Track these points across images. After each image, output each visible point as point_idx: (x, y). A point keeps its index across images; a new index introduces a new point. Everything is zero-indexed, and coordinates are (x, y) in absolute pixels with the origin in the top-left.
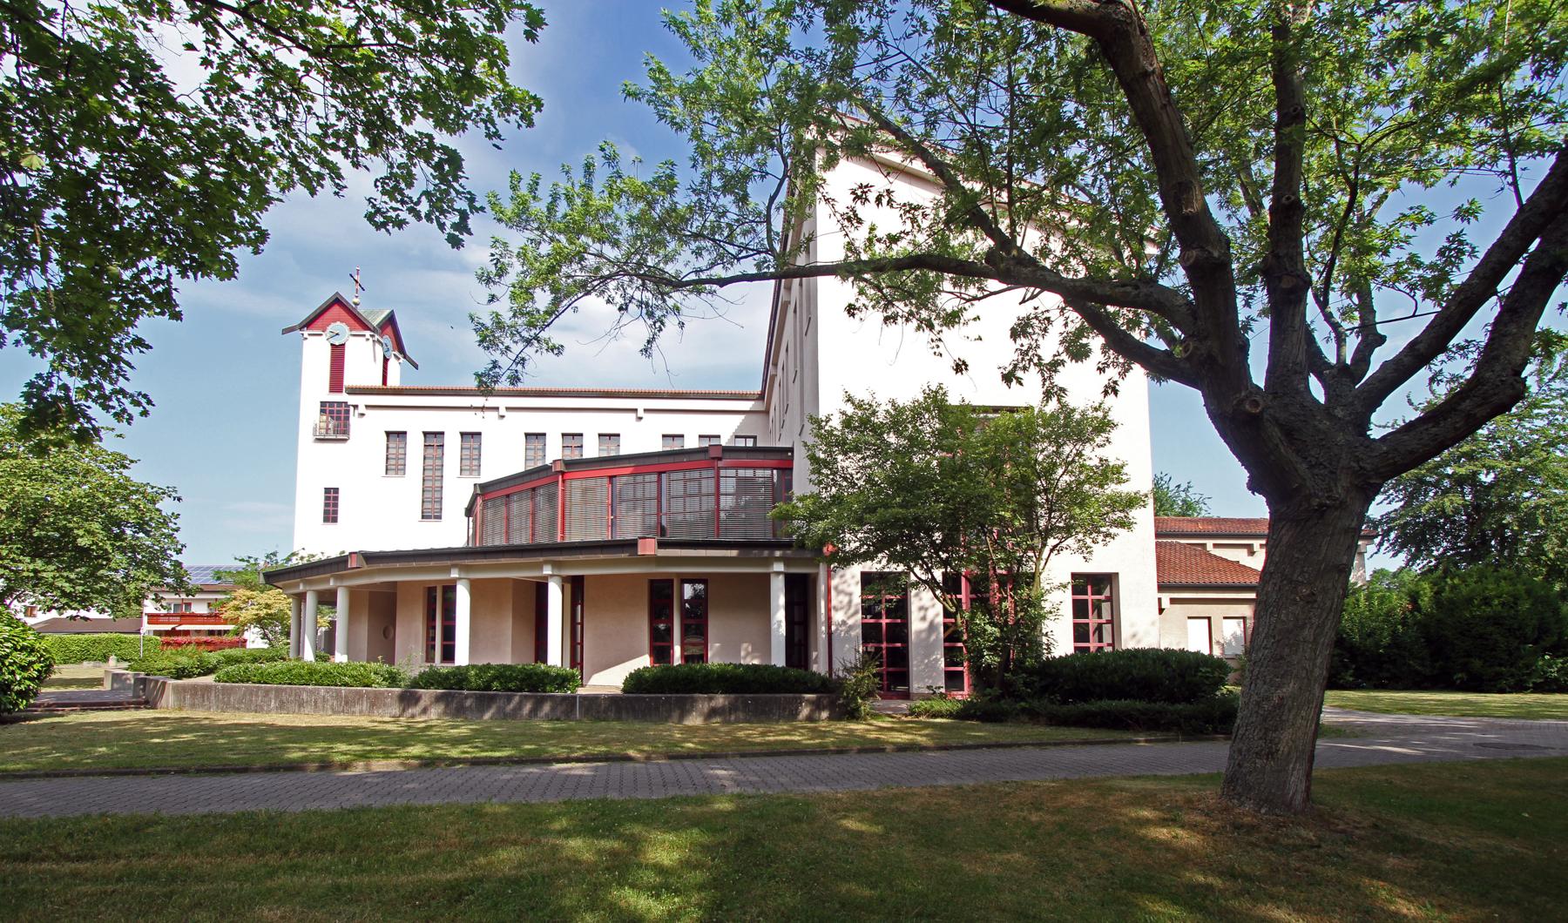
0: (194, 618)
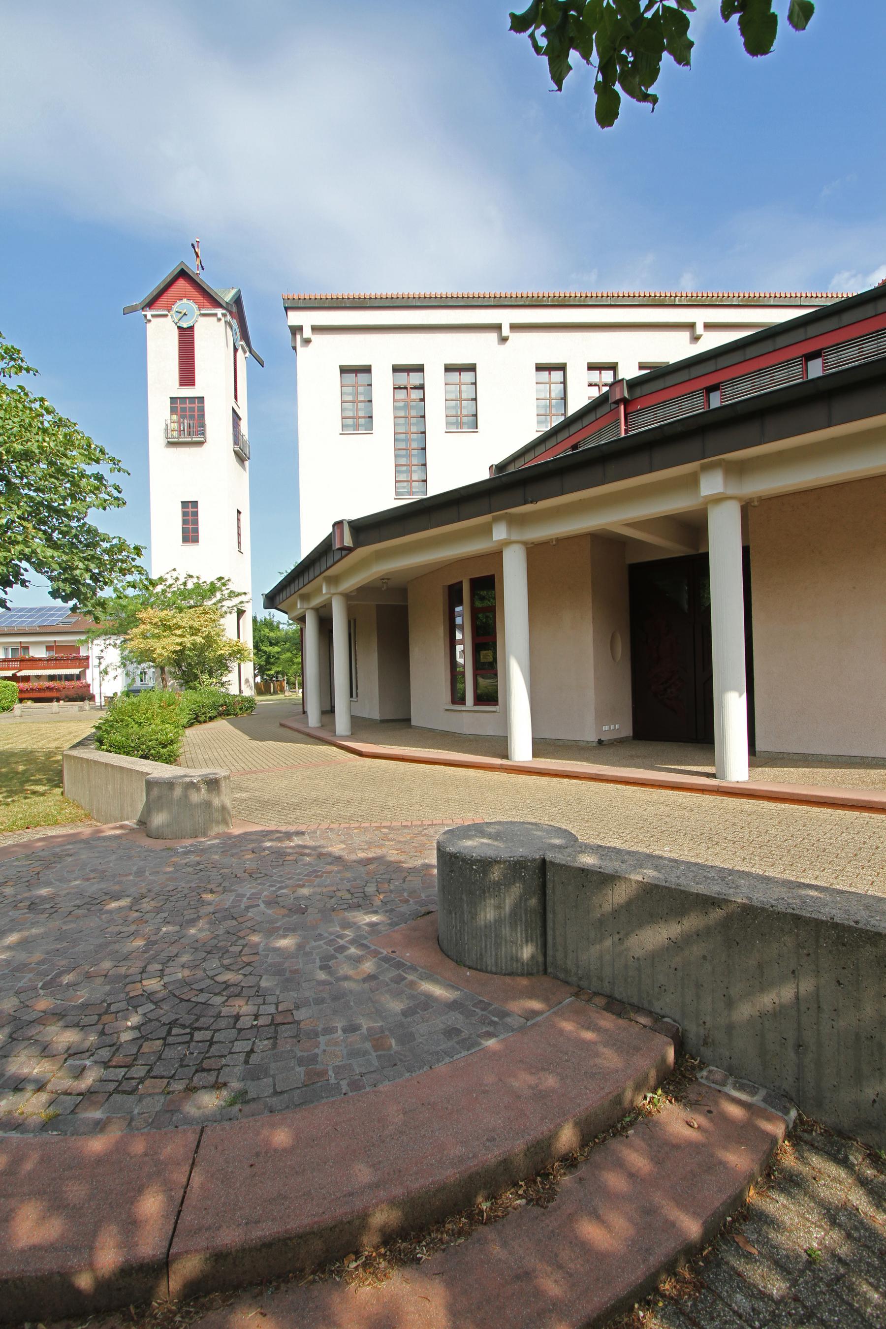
0: (34, 662)
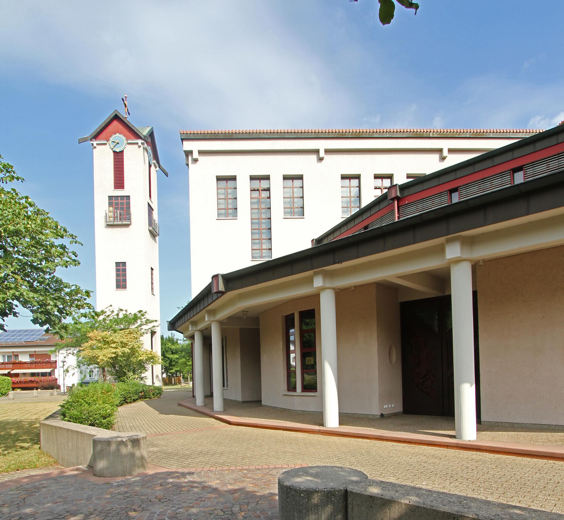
0: (22, 365)
